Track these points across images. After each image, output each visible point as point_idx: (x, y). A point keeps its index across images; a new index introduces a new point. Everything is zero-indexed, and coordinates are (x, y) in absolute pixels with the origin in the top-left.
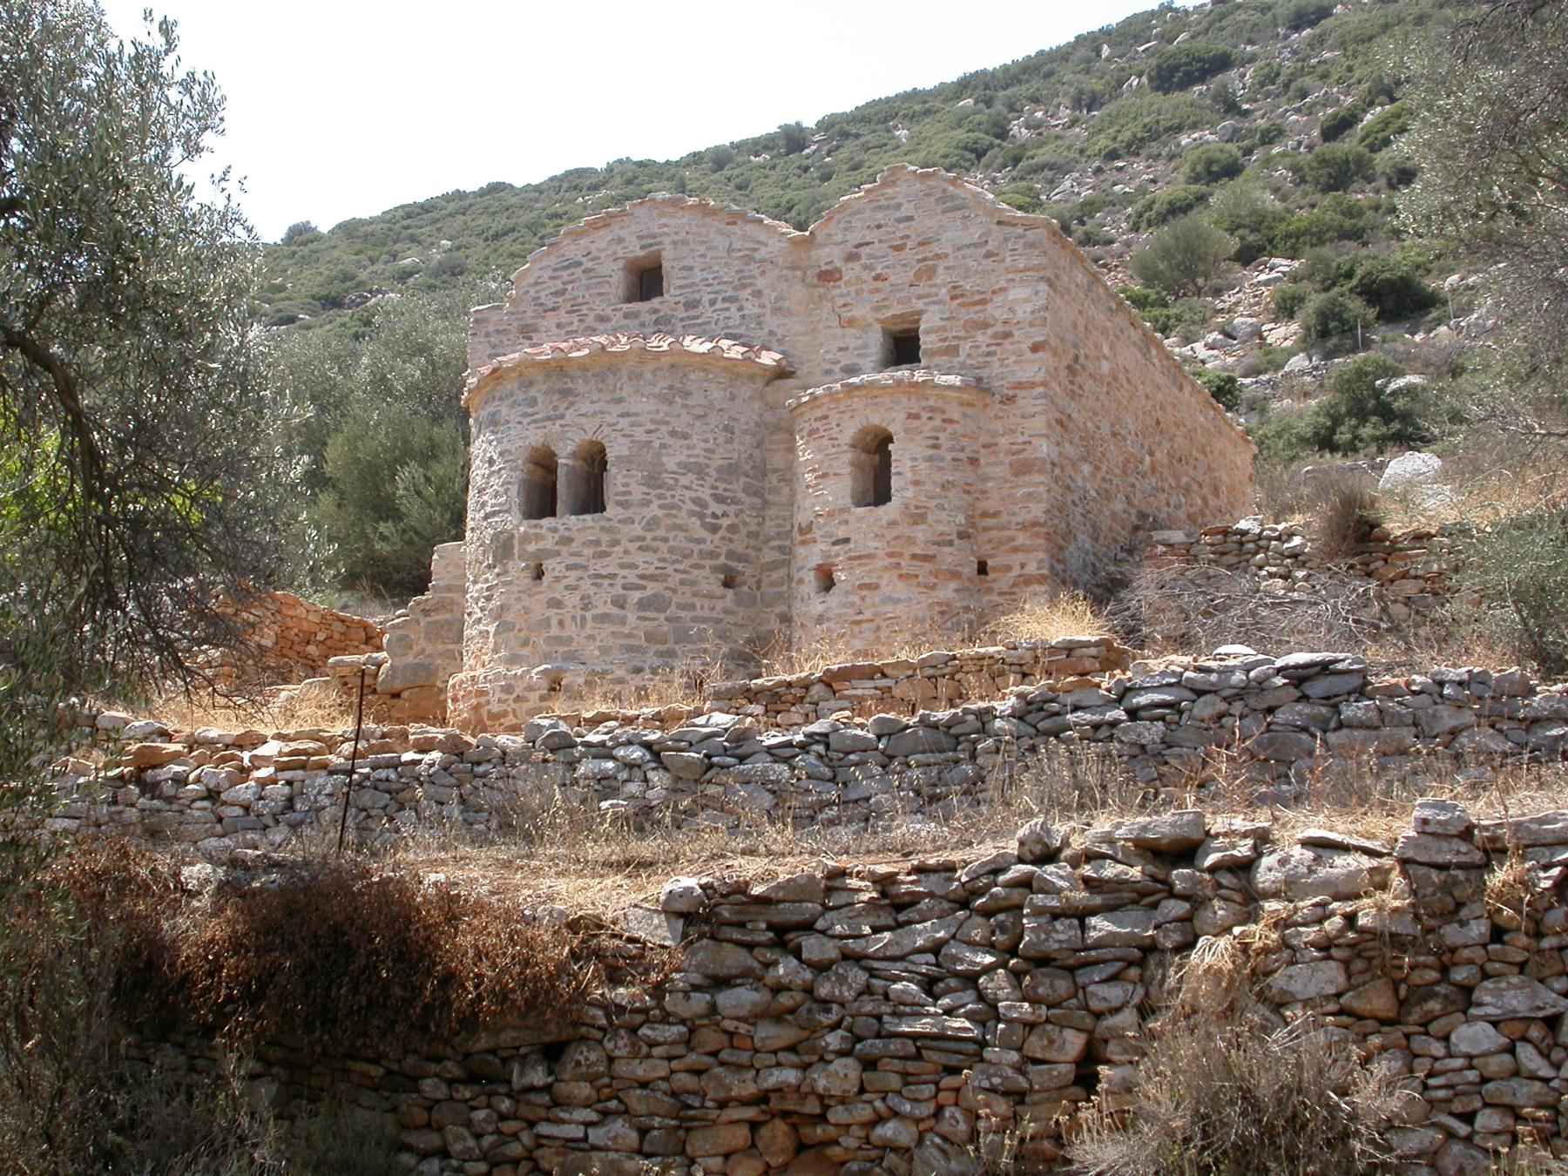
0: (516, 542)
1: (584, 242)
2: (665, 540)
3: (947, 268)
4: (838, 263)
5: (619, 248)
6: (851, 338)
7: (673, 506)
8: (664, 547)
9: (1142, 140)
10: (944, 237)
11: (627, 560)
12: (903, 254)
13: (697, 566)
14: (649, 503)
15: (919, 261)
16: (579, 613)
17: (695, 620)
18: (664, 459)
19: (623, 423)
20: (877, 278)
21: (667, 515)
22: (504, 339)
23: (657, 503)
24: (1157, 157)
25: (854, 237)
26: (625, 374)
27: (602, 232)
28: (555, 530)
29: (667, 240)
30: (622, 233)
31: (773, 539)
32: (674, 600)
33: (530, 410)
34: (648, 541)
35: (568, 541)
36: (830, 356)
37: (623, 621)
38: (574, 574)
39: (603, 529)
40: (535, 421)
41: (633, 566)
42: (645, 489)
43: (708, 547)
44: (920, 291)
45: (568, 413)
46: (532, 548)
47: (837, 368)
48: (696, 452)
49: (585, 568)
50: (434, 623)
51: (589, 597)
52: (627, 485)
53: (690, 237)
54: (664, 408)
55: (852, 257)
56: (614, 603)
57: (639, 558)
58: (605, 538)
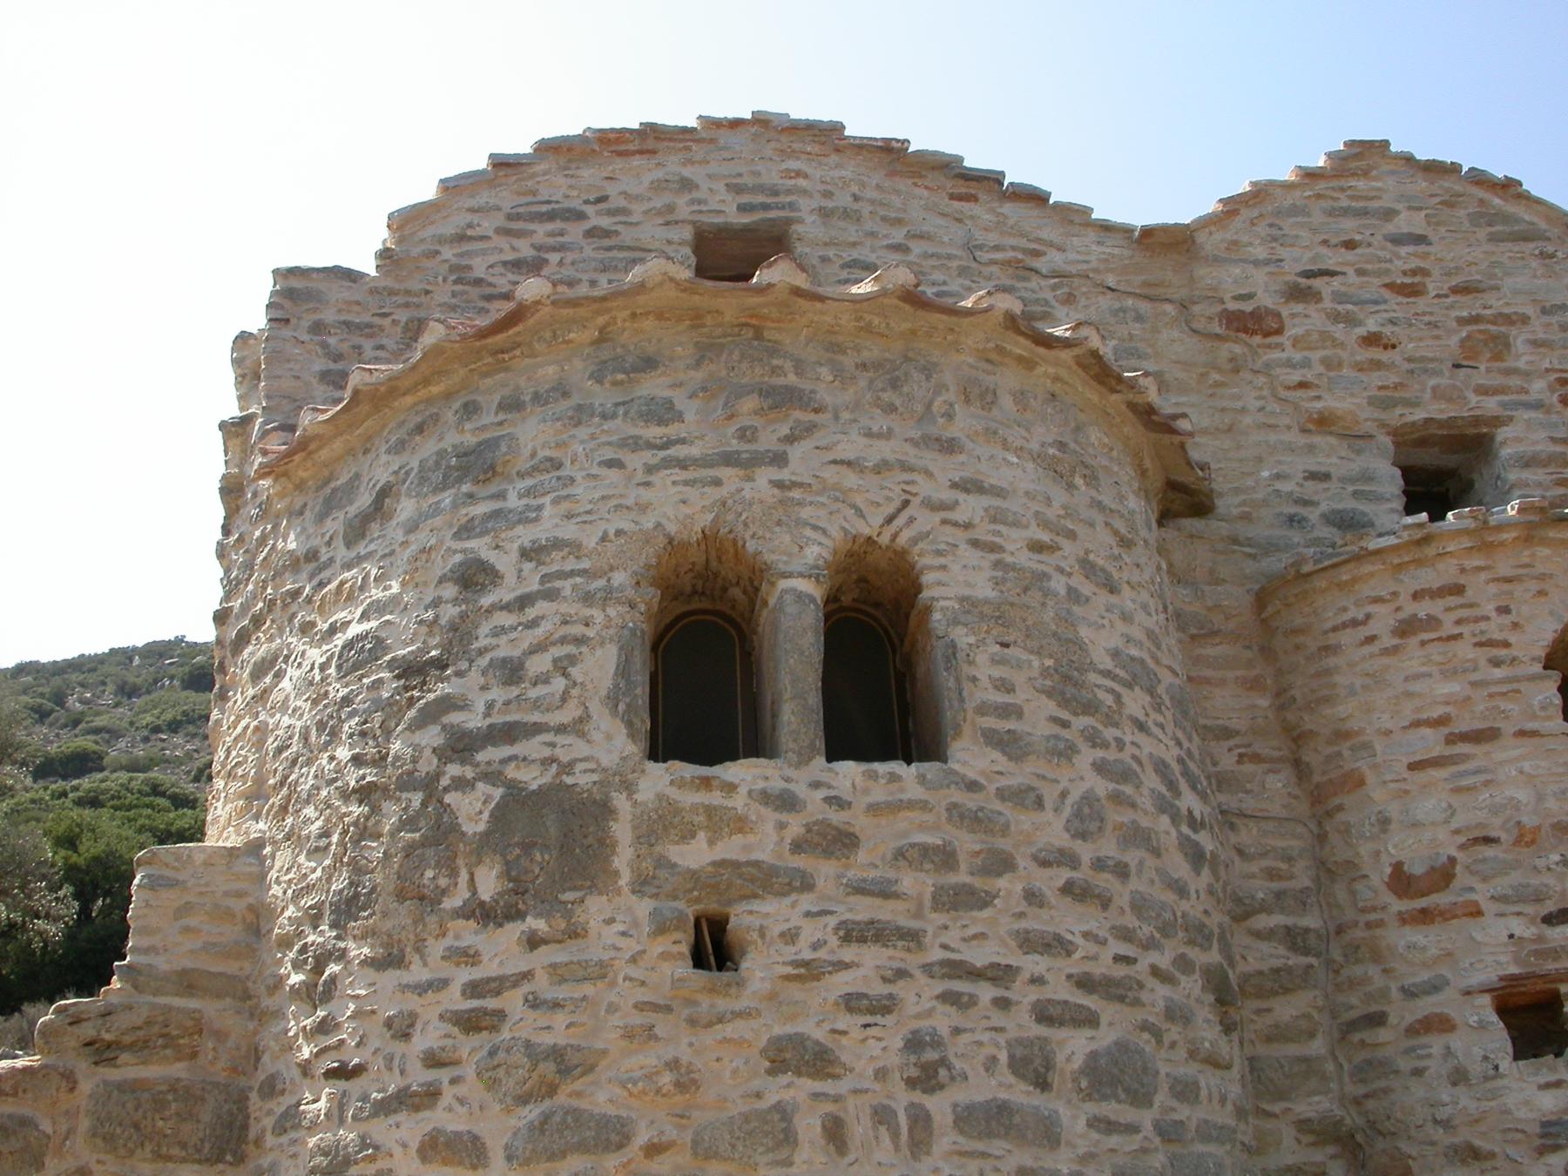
0: (622, 830)
1: (589, 174)
2: (1122, 872)
3: (1536, 344)
4: (1266, 300)
5: (682, 201)
6: (1331, 454)
7: (1126, 776)
8: (1122, 894)
9: (181, 721)
10: (1508, 283)
11: (1037, 922)
12: (1421, 304)
13: (1183, 963)
14: (1066, 753)
15: (1462, 321)
16: (901, 1099)
17: (1207, 1132)
18: (1084, 632)
19: (971, 507)
20: (1372, 340)
21: (1117, 798)
22: (368, 345)
23: (1087, 756)
24: (194, 736)
25: (1296, 259)
26: (948, 378)
27: (637, 161)
28: (786, 802)
29: (805, 204)
30: (687, 172)
31: (1264, 908)
32: (1163, 1069)
33: (654, 432)
34: (1083, 874)
35: (840, 842)
36: (1286, 487)
37: (1049, 1134)
38: (872, 959)
39: (956, 813)
40: (683, 464)
41: (1056, 945)
42: (1050, 707)
43: (1192, 908)
44: (1480, 378)
45: (796, 452)
46: (695, 854)
47: (1313, 515)
48: (1138, 634)
49: (913, 938)
50: (121, 1087)
51: (937, 1043)
52: (1005, 686)
53: (866, 209)
54: (1059, 496)
55: (1297, 293)
56: (1019, 1066)
57: (1071, 920)
58: (967, 843)
